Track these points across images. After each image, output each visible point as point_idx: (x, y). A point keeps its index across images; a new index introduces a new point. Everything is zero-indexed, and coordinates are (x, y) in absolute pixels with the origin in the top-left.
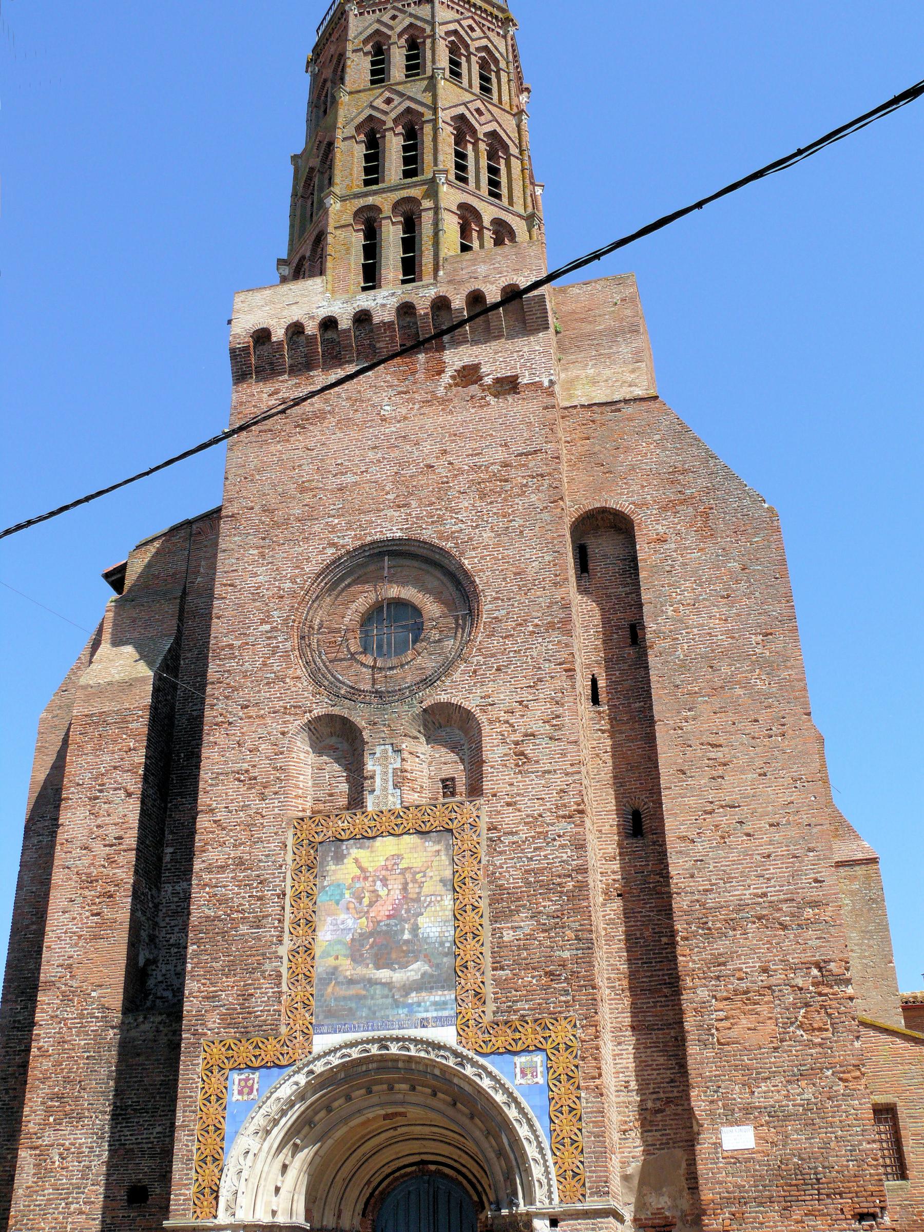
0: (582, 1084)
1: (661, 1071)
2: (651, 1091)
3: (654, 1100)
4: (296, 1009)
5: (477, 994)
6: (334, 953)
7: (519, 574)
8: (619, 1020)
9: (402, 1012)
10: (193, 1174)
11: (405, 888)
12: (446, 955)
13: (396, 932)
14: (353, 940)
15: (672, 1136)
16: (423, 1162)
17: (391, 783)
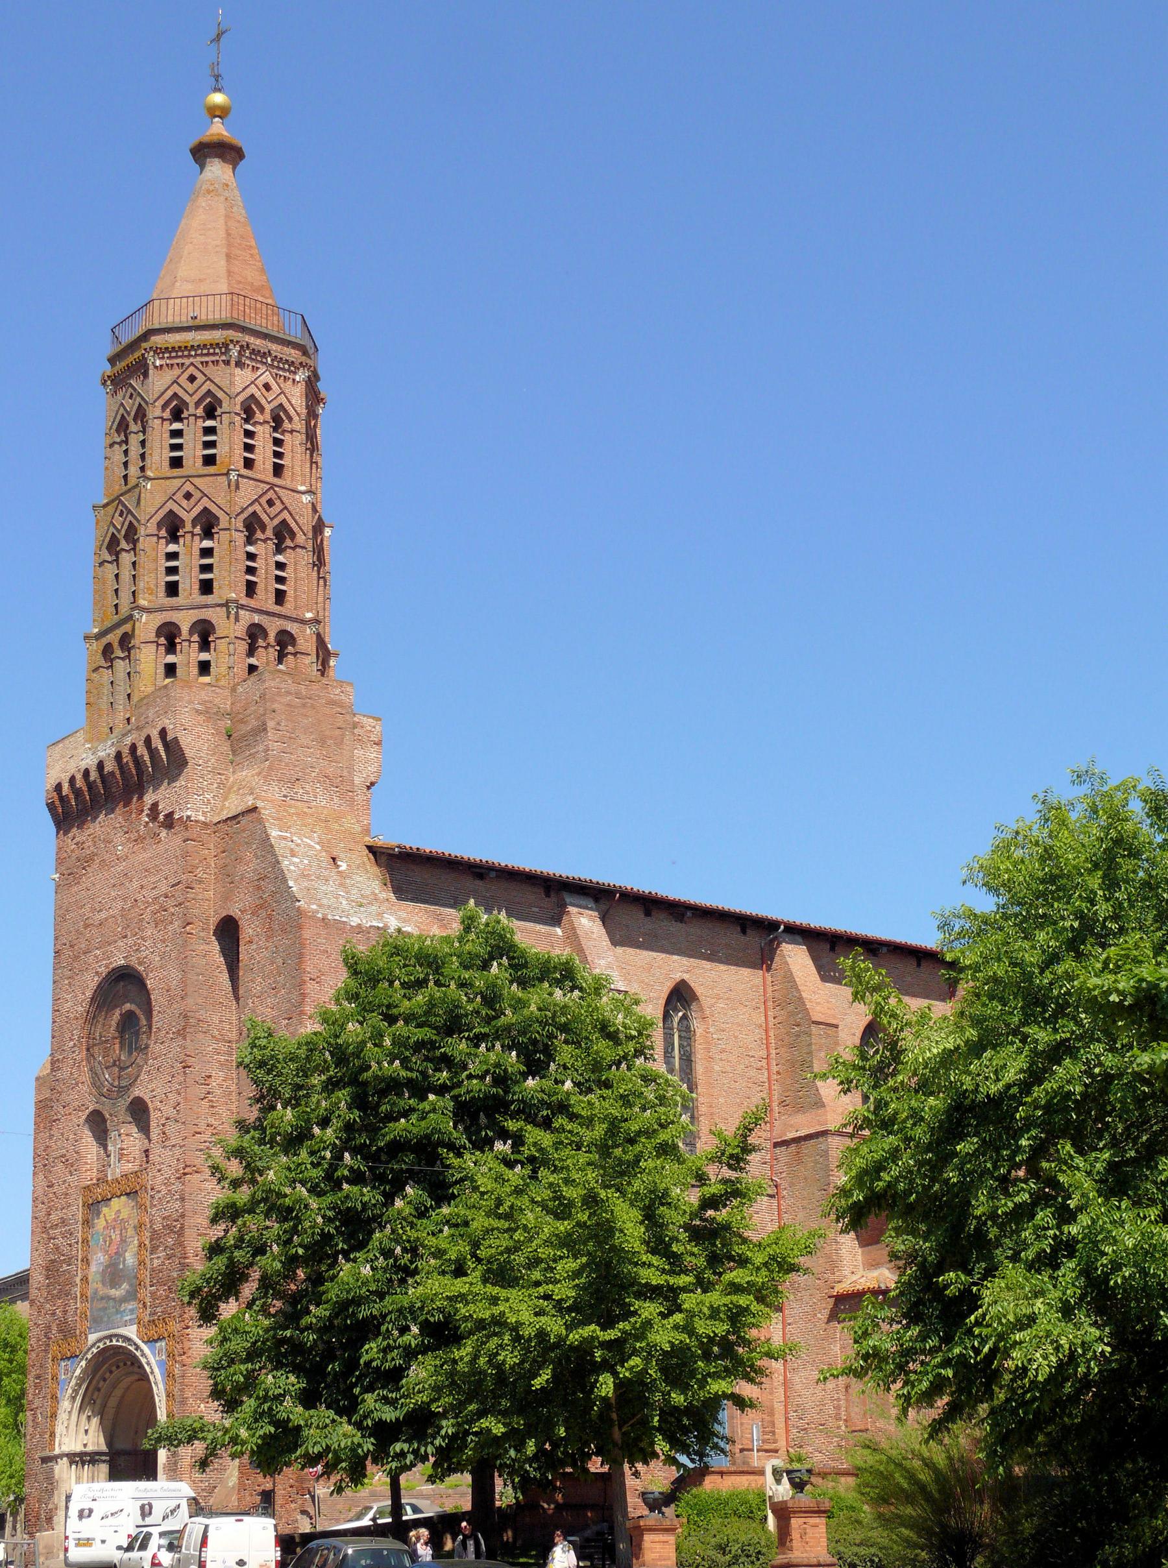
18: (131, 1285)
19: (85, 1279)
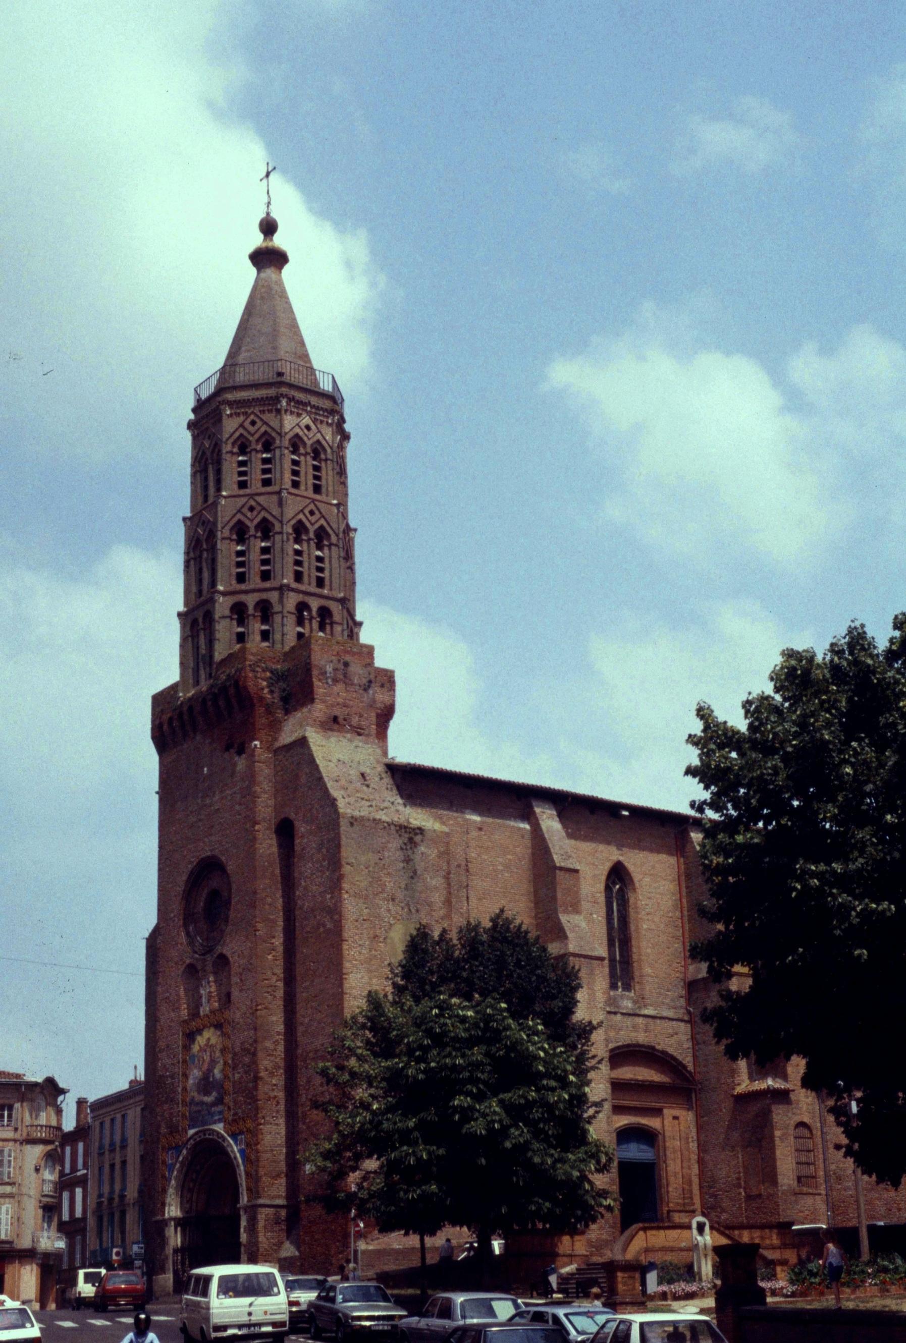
19: (185, 1089)
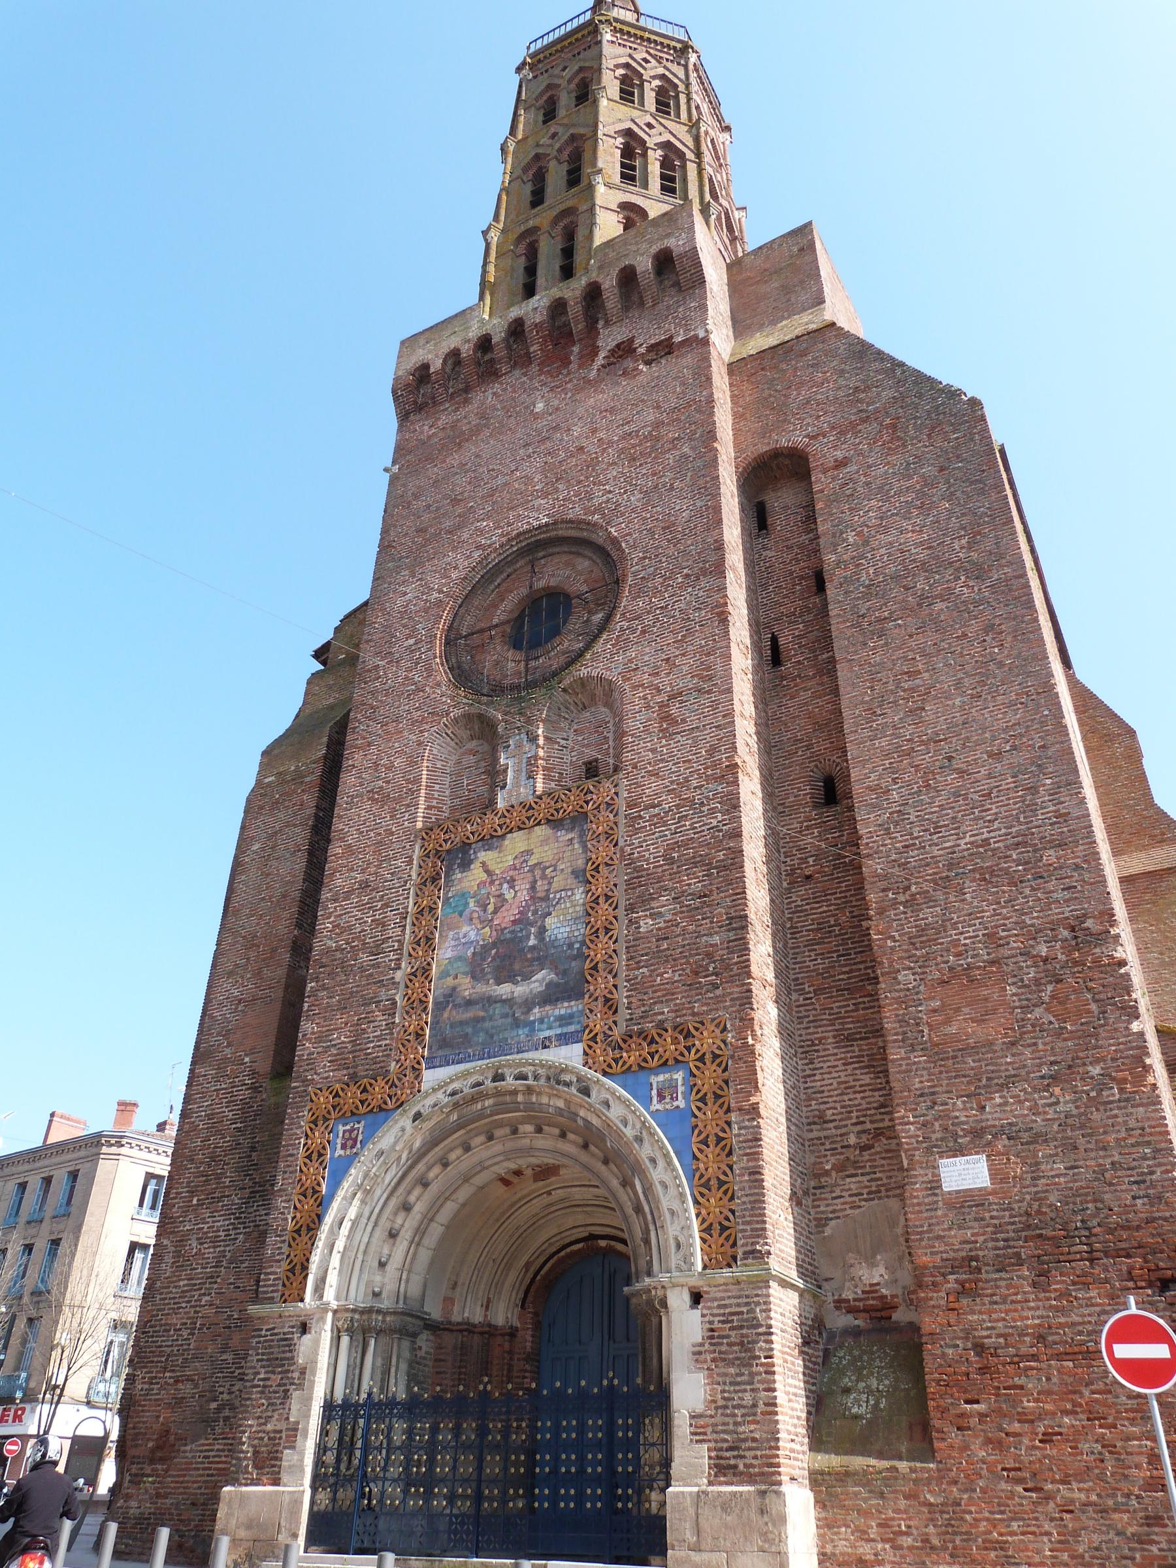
0: (732, 1105)
1: (867, 1094)
2: (854, 1121)
3: (859, 1132)
4: (409, 1041)
5: (607, 1000)
6: (452, 972)
7: (668, 527)
8: (811, 1031)
9: (522, 1032)
10: (285, 1249)
11: (533, 888)
12: (575, 958)
13: (521, 940)
14: (474, 954)
15: (885, 1181)
16: (593, 1237)
17: (524, 774)
18: (565, 973)
